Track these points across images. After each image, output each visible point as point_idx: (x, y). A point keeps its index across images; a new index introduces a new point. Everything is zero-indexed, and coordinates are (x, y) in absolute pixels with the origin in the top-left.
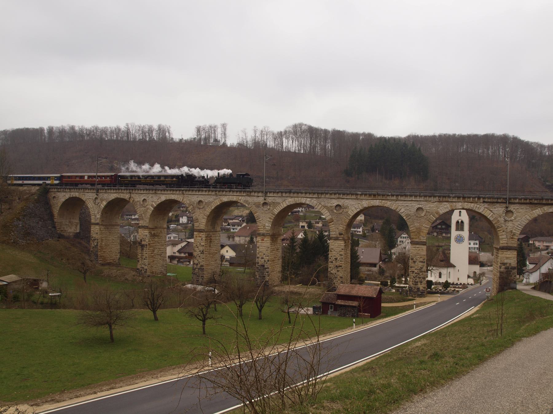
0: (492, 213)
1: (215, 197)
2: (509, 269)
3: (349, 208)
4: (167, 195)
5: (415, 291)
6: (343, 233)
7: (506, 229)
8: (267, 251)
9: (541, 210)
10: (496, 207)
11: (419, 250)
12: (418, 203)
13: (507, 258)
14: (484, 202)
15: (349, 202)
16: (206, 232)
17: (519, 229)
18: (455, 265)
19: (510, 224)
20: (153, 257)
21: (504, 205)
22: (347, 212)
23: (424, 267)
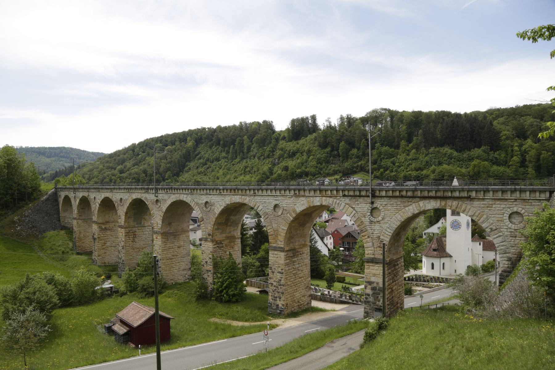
0: (354, 212)
1: (128, 194)
2: (376, 290)
3: (216, 205)
4: (105, 193)
5: (274, 308)
6: (211, 234)
7: (372, 233)
8: (159, 249)
9: (416, 207)
10: (358, 202)
11: (277, 258)
12: (275, 199)
13: (374, 275)
14: (344, 196)
15: (214, 199)
16: (125, 228)
17: (387, 234)
18: (452, 255)
19: (377, 227)
20: (104, 249)
21: (369, 200)
22: (213, 210)
23: (283, 280)
